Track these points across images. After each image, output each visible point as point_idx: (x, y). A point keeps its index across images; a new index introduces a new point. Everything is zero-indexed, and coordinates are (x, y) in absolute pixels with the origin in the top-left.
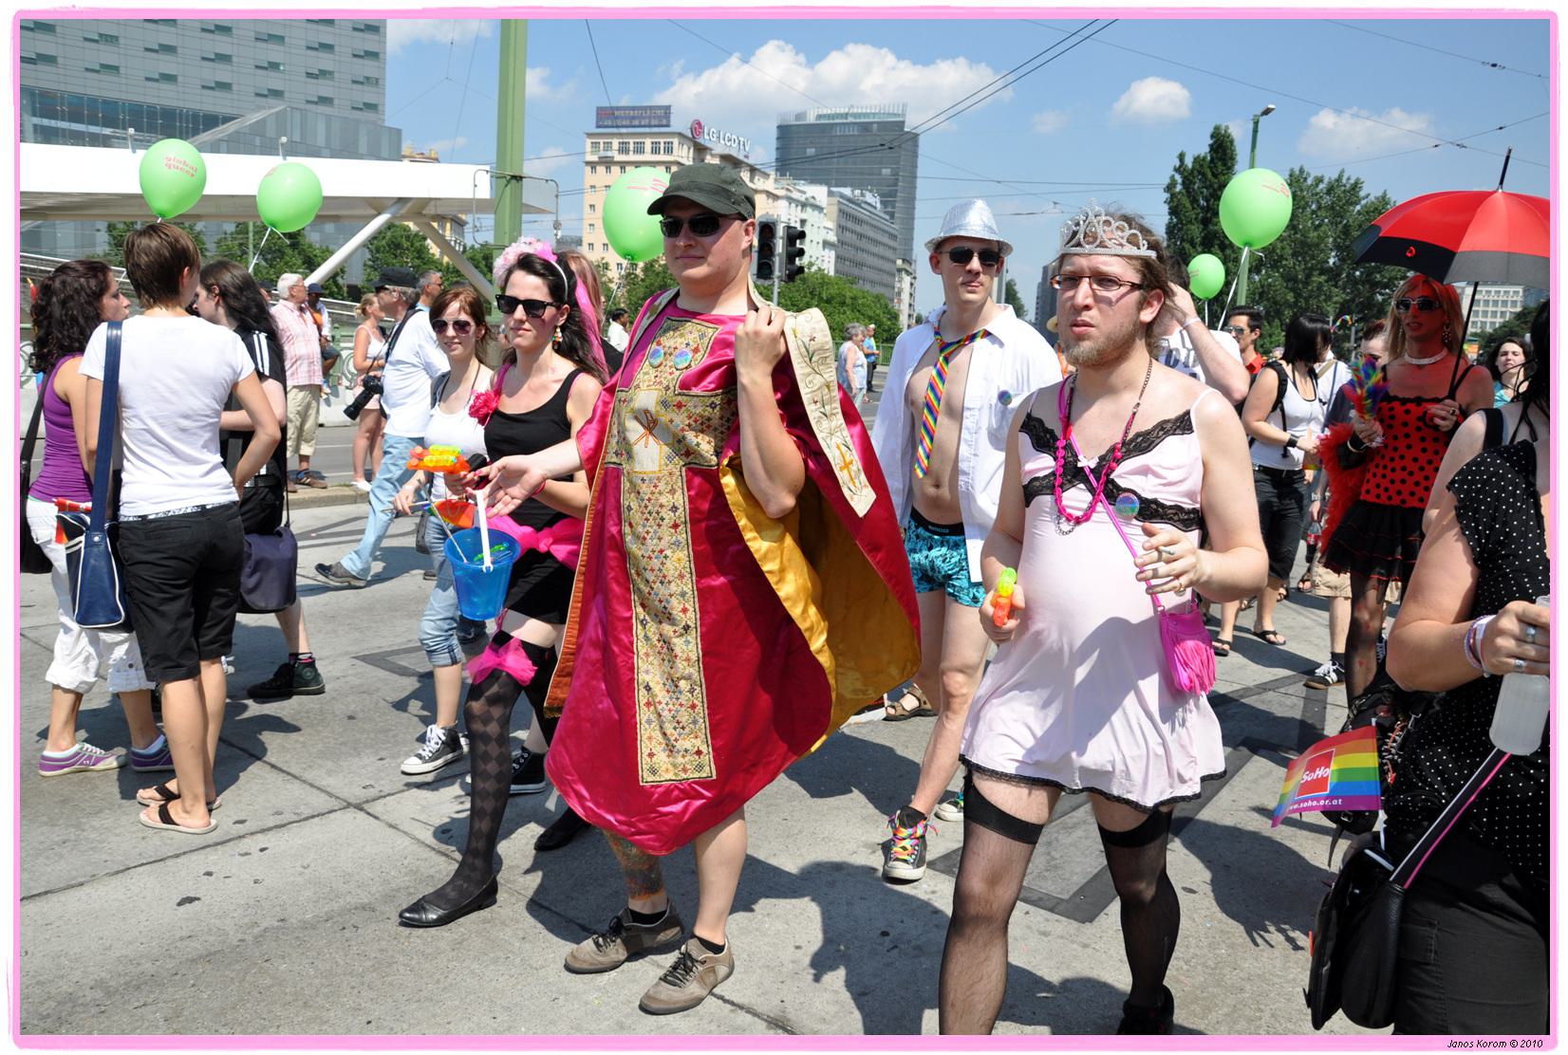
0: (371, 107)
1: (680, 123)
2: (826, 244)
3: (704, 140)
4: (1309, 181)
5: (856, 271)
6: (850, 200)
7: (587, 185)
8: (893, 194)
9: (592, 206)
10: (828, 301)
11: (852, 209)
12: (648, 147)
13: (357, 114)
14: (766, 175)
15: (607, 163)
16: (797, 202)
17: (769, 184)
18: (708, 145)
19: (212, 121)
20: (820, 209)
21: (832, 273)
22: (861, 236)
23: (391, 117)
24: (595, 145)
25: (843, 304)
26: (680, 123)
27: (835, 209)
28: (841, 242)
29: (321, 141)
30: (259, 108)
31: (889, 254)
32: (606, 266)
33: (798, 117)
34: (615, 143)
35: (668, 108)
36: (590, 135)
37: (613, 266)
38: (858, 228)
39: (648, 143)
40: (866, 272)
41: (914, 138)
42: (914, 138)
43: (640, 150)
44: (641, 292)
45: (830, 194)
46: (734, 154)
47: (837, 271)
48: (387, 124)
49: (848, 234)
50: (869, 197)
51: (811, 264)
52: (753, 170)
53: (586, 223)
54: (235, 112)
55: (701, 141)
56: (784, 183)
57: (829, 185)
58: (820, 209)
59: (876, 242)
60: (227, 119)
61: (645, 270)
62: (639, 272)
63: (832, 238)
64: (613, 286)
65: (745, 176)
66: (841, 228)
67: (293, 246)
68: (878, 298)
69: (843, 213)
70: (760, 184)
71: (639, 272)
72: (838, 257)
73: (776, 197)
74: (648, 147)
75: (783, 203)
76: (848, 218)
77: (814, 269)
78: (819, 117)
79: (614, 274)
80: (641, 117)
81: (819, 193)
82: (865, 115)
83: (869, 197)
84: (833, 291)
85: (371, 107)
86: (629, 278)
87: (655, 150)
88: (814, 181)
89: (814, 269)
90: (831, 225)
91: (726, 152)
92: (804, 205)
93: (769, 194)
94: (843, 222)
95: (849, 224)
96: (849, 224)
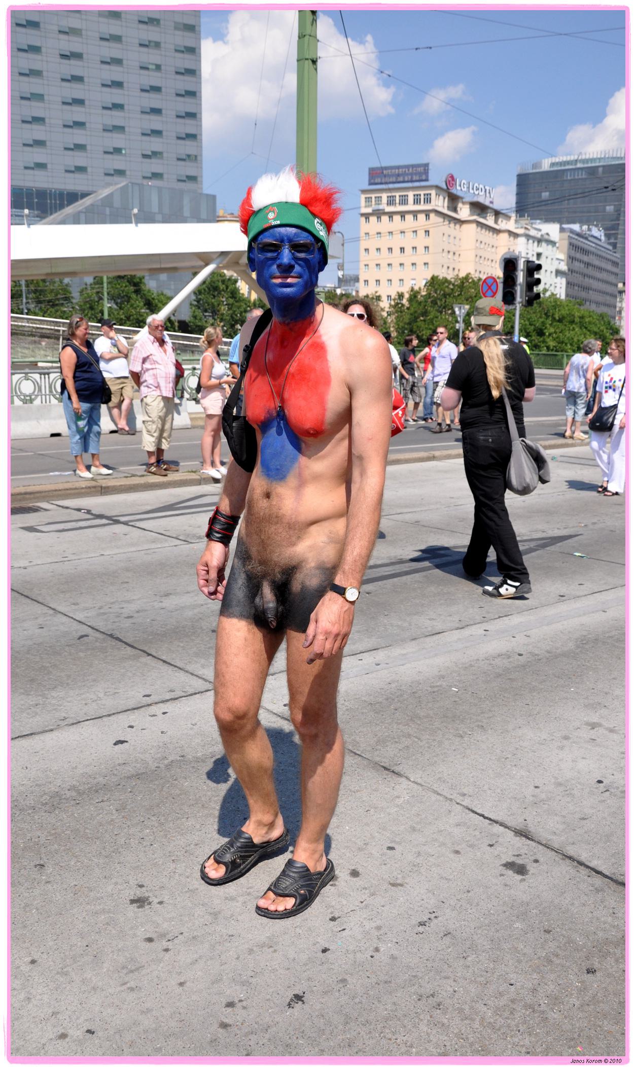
0: (193, 179)
1: (437, 177)
2: (558, 273)
3: (457, 190)
7: (362, 234)
9: (367, 250)
10: (560, 321)
12: (411, 199)
13: (182, 185)
14: (508, 217)
15: (379, 214)
17: (511, 225)
18: (459, 194)
19: (73, 197)
20: (553, 243)
21: (563, 297)
23: (208, 186)
24: (368, 200)
25: (572, 322)
26: (437, 177)
28: (571, 270)
29: (155, 209)
30: (109, 184)
32: (378, 298)
33: (535, 166)
34: (384, 196)
35: (427, 165)
36: (364, 192)
37: (384, 298)
39: (411, 195)
43: (404, 201)
44: (407, 318)
45: (562, 230)
46: (481, 200)
47: (567, 295)
51: (545, 290)
52: (497, 213)
54: (90, 189)
55: (454, 191)
56: (524, 222)
57: (561, 223)
58: (553, 243)
60: (84, 195)
61: (410, 300)
62: (405, 302)
63: (564, 267)
64: (385, 314)
65: (490, 221)
66: (571, 259)
67: (137, 292)
69: (572, 246)
70: (503, 224)
71: (405, 302)
72: (568, 283)
73: (516, 235)
74: (411, 199)
75: (522, 240)
77: (548, 294)
78: (553, 164)
79: (385, 304)
80: (404, 174)
81: (552, 230)
84: (564, 312)
85: (193, 179)
86: (397, 307)
87: (417, 201)
88: (548, 220)
89: (548, 294)
90: (562, 256)
91: (475, 199)
92: (539, 241)
94: (573, 253)
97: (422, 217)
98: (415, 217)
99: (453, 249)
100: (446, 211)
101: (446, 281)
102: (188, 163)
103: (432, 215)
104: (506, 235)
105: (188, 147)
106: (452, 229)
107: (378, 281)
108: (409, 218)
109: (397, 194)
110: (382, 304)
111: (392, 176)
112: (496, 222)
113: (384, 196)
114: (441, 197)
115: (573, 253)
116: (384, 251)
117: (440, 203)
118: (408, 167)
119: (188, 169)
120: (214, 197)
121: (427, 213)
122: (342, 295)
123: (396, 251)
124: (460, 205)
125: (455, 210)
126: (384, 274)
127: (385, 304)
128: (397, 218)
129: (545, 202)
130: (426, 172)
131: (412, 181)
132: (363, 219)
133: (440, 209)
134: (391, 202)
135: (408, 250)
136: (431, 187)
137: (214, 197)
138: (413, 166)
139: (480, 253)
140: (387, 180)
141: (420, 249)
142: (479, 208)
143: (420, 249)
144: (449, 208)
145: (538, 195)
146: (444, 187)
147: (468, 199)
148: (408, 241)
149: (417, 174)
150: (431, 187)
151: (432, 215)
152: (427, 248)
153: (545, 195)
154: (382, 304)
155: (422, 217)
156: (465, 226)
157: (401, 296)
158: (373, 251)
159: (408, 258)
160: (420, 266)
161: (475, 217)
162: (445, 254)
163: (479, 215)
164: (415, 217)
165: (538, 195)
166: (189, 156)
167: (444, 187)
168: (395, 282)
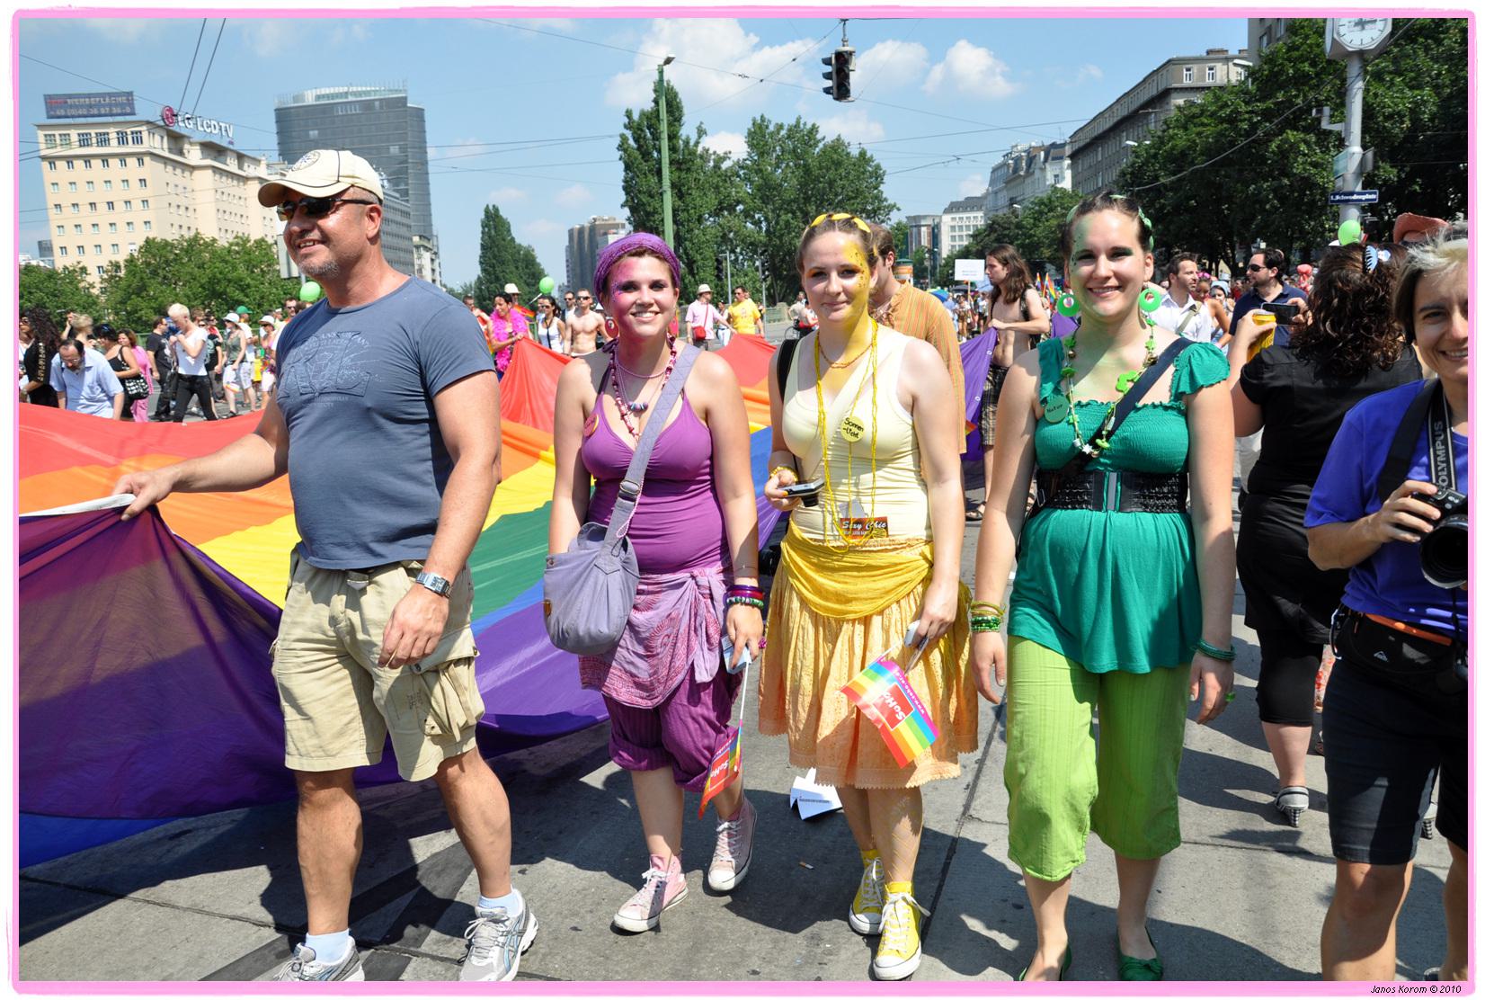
1: (148, 109)
3: (180, 127)
4: (772, 128)
12: (114, 142)
14: (256, 161)
18: (183, 132)
26: (148, 109)
31: (403, 231)
37: (92, 270)
46: (216, 140)
52: (240, 157)
55: (175, 128)
64: (95, 291)
65: (232, 165)
70: (249, 170)
71: (122, 273)
79: (94, 278)
86: (112, 280)
91: (208, 139)
97: (132, 162)
99: (184, 202)
100: (166, 154)
101: (166, 244)
103: (147, 159)
106: (178, 177)
108: (114, 162)
109: (93, 132)
112: (241, 167)
114: (157, 137)
117: (157, 143)
121: (140, 157)
123: (102, 207)
124: (187, 146)
125: (181, 153)
127: (94, 278)
128: (96, 163)
130: (131, 103)
131: (112, 115)
135: (119, 206)
136: (141, 123)
139: (223, 207)
141: (137, 204)
143: (137, 204)
144: (170, 150)
148: (117, 193)
150: (141, 123)
151: (147, 159)
152: (145, 202)
156: (196, 173)
157: (117, 266)
159: (121, 214)
160: (139, 224)
162: (173, 209)
163: (215, 159)
168: (107, 249)
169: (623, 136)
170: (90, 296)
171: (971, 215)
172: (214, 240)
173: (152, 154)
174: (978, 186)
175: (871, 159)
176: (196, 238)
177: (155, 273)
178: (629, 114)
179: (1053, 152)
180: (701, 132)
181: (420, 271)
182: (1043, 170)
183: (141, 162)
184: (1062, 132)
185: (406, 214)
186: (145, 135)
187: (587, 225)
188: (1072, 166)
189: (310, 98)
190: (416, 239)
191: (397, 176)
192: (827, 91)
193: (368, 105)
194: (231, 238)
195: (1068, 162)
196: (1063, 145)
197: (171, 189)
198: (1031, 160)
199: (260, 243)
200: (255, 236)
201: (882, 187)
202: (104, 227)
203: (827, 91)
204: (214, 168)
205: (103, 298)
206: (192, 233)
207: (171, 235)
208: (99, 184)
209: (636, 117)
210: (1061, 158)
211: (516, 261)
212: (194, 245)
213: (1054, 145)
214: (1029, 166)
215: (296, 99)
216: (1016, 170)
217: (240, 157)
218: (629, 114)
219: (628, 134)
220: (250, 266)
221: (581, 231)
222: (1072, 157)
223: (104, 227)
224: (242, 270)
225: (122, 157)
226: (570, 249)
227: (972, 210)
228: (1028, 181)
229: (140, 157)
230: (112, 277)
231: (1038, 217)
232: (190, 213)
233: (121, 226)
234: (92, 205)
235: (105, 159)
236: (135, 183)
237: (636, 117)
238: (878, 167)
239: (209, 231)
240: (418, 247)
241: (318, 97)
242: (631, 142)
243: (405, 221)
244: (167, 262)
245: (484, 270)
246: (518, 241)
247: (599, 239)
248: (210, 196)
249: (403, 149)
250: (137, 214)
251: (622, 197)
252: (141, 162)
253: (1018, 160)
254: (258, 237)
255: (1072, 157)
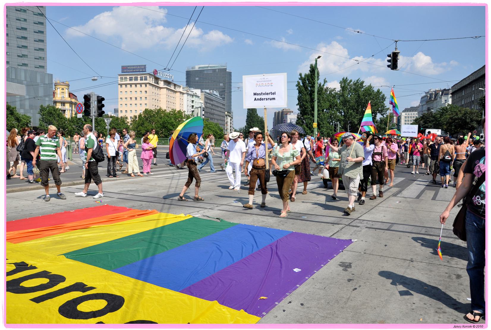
1: (150, 70)
3: (158, 76)
5: (212, 116)
6: (208, 94)
8: (224, 91)
11: (209, 97)
12: (139, 79)
14: (180, 87)
16: (190, 95)
17: (181, 90)
18: (159, 77)
20: (198, 97)
22: (213, 105)
24: (122, 78)
27: (203, 97)
31: (223, 110)
35: (145, 66)
36: (119, 75)
37: (129, 118)
38: (211, 103)
39: (139, 77)
40: (215, 117)
41: (230, 73)
42: (230, 73)
43: (136, 79)
45: (202, 92)
46: (169, 80)
48: (48, 73)
49: (208, 105)
50: (215, 93)
52: (175, 85)
53: (120, 103)
55: (157, 76)
57: (202, 88)
59: (218, 107)
64: (129, 124)
65: (172, 88)
66: (206, 103)
68: (216, 124)
70: (177, 89)
71: (137, 119)
73: (183, 93)
74: (139, 79)
75: (185, 95)
76: (207, 99)
79: (129, 120)
80: (136, 69)
81: (198, 92)
82: (212, 67)
83: (215, 93)
86: (134, 121)
87: (141, 79)
88: (196, 88)
90: (202, 102)
92: (193, 96)
93: (181, 92)
94: (206, 101)
95: (209, 101)
96: (209, 101)
97: (143, 86)
98: (141, 86)
99: (157, 98)
100: (154, 84)
102: (39, 60)
103: (148, 85)
104: (179, 93)
105: (40, 54)
107: (126, 111)
108: (138, 86)
110: (128, 120)
111: (131, 69)
112: (175, 88)
113: (128, 77)
114: (151, 79)
115: (206, 101)
116: (129, 99)
117: (151, 80)
118: (137, 66)
119: (41, 63)
120: (51, 75)
121: (146, 84)
122: (111, 117)
123: (134, 99)
124: (159, 82)
125: (158, 83)
126: (128, 108)
127: (129, 120)
129: (197, 82)
132: (119, 86)
133: (151, 83)
134: (131, 79)
135: (138, 98)
137: (51, 75)
138: (139, 66)
140: (129, 71)
141: (143, 98)
142: (167, 83)
143: (143, 98)
145: (194, 79)
146: (152, 73)
147: (163, 79)
148: (138, 95)
149: (141, 69)
151: (148, 85)
153: (197, 79)
154: (128, 120)
155: (143, 86)
157: (136, 117)
158: (124, 99)
159: (138, 102)
160: (143, 105)
161: (165, 86)
164: (141, 86)
165: (194, 79)
166: (40, 57)
167: (152, 73)
169: (299, 83)
170: (127, 125)
171: (413, 113)
172: (165, 110)
173: (149, 84)
174: (416, 103)
175: (381, 93)
176: (160, 109)
177: (147, 119)
178: (300, 75)
179: (445, 92)
180: (325, 81)
181: (227, 123)
182: (441, 98)
183: (146, 86)
184: (449, 86)
185: (224, 105)
186: (148, 76)
187: (281, 111)
188: (452, 97)
189: (197, 68)
190: (226, 113)
191: (222, 93)
192: (389, 66)
193: (214, 70)
194: (170, 110)
195: (450, 95)
196: (449, 90)
197: (154, 94)
198: (436, 94)
199: (179, 112)
200: (178, 109)
201: (385, 102)
202: (133, 105)
203: (389, 66)
204: (167, 88)
205: (131, 127)
206: (159, 108)
207: (153, 108)
208: (134, 92)
209: (303, 76)
210: (448, 94)
211: (258, 121)
212: (159, 111)
213: (445, 90)
214: (435, 97)
215: (192, 68)
216: (430, 98)
217: (175, 85)
218: (300, 75)
219: (300, 81)
220: (175, 119)
221: (279, 113)
222: (452, 94)
223: (133, 105)
224: (173, 120)
225: (141, 84)
226: (275, 118)
227: (413, 111)
228: (435, 102)
229: (146, 84)
230: (134, 120)
231: (442, 114)
232: (159, 102)
233: (138, 105)
234: (131, 98)
235: (136, 85)
236: (144, 92)
237: (303, 76)
238: (384, 95)
239: (164, 107)
240: (226, 115)
241: (199, 68)
242: (301, 84)
243: (223, 107)
244: (151, 116)
245: (247, 124)
246: (259, 115)
247: (284, 116)
248: (165, 96)
249: (224, 84)
250: (144, 101)
251: (297, 102)
252: (146, 86)
253: (431, 94)
254: (179, 110)
255: (452, 94)
